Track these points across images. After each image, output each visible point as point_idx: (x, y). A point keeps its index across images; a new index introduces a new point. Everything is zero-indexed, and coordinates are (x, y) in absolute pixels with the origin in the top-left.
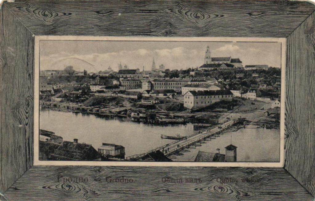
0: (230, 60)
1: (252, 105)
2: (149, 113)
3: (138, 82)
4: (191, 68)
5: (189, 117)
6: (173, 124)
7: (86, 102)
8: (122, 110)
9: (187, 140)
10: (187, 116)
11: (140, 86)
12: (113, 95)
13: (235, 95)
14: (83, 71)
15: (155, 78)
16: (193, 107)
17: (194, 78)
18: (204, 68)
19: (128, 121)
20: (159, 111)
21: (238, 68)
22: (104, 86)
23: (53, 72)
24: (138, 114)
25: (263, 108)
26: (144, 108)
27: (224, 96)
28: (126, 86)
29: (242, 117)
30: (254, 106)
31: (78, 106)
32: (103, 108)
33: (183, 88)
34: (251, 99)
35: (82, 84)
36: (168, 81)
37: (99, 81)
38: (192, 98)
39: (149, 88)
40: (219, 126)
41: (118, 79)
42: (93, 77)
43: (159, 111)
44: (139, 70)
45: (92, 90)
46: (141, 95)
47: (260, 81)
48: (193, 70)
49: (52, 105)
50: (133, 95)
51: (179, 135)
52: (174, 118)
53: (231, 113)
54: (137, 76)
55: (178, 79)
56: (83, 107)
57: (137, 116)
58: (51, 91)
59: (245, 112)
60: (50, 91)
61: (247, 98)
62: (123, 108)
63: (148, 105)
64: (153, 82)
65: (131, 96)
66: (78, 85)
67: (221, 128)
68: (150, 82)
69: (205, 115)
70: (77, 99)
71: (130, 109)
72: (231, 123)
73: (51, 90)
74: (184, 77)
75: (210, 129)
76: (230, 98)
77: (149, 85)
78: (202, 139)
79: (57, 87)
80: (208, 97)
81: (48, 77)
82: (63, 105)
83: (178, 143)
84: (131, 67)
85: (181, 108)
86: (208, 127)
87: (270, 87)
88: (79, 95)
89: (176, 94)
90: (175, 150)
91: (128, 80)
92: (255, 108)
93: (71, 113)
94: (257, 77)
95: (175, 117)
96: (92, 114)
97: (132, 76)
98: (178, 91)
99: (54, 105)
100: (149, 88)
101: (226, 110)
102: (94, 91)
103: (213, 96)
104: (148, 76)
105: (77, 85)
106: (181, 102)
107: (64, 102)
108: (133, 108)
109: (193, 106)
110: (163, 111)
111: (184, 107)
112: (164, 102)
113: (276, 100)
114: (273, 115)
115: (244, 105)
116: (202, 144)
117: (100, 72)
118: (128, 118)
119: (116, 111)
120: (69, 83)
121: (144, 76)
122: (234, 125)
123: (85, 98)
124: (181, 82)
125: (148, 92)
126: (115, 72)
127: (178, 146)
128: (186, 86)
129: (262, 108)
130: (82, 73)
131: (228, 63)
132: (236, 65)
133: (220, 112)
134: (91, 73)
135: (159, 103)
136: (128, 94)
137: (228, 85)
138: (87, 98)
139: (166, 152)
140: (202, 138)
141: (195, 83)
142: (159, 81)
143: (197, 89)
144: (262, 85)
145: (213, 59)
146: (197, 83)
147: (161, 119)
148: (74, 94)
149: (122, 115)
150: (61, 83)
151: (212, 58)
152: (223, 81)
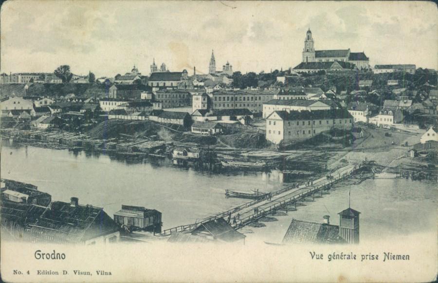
0: (349, 55)
1: (386, 137)
2: (204, 151)
3: (186, 95)
4: (280, 70)
5: (274, 159)
6: (247, 171)
7: (92, 131)
8: (157, 145)
9: (272, 199)
10: (272, 156)
11: (188, 102)
12: (140, 118)
13: (357, 119)
14: (86, 74)
15: (215, 88)
16: (281, 141)
17: (285, 88)
18: (301, 71)
19: (167, 166)
20: (221, 148)
21: (362, 69)
22: (124, 103)
23: (33, 76)
24: (185, 154)
25: (407, 143)
26: (196, 142)
27: (337, 121)
28: (164, 101)
29: (369, 159)
30: (390, 138)
31: (79, 138)
32: (123, 142)
33: (264, 106)
34: (385, 127)
35: (86, 99)
36: (239, 94)
37: (115, 92)
38: (280, 124)
39: (204, 106)
40: (328, 174)
41: (149, 89)
42: (106, 86)
43: (221, 148)
44: (187, 72)
45: (104, 110)
46: (191, 118)
47: (401, 94)
48: (282, 74)
49: (31, 136)
50: (178, 118)
51: (258, 190)
52: (248, 161)
53: (350, 151)
54: (183, 84)
55: (256, 89)
56: (88, 140)
57: (183, 157)
58: (31, 110)
59: (374, 149)
60: (28, 111)
61: (378, 125)
62: (158, 142)
63: (203, 137)
64: (211, 96)
65: (172, 120)
66: (79, 99)
67: (331, 178)
68: (205, 95)
69: (305, 154)
70: (76, 125)
71: (172, 144)
72: (349, 169)
73: (30, 109)
74: (267, 86)
75: (312, 180)
76: (346, 124)
77: (204, 100)
78: (298, 198)
79: (41, 103)
80: (309, 122)
81: (24, 85)
82: (51, 136)
83: (256, 206)
84: (172, 68)
85: (261, 141)
86: (309, 176)
87: (418, 106)
88: (80, 118)
89: (252, 117)
90: (251, 217)
91: (167, 92)
92: (393, 142)
93: (67, 151)
94: (395, 85)
95: (250, 158)
96: (105, 153)
97: (175, 83)
98: (256, 111)
99: (35, 135)
100: (204, 106)
101: (340, 145)
102: (107, 110)
103: (317, 122)
104: (202, 84)
105: (77, 100)
106: (261, 132)
107: (53, 130)
108: (175, 143)
109: (282, 138)
110: (229, 148)
111: (266, 140)
112: (231, 131)
113: (429, 128)
114: (424, 155)
115: (373, 137)
116: (297, 208)
117: (118, 77)
118: (167, 160)
119: (147, 148)
120: (62, 97)
121: (195, 84)
122: (356, 172)
123: (90, 124)
124: (261, 96)
125: (203, 112)
126: (143, 77)
127: (256, 210)
128: (267, 103)
129: (404, 143)
130: (85, 78)
131: (345, 61)
132: (359, 64)
133: (330, 149)
134: (103, 78)
135: (223, 133)
136: (168, 116)
137: (343, 101)
138: (95, 123)
139: (235, 222)
140: (298, 196)
141: (286, 97)
142: (222, 93)
143: (289, 108)
144: (405, 101)
145: (319, 54)
146: (290, 97)
147: (226, 162)
148: (70, 116)
149: (156, 155)
150: (48, 97)
151: (316, 52)
152: (335, 94)
